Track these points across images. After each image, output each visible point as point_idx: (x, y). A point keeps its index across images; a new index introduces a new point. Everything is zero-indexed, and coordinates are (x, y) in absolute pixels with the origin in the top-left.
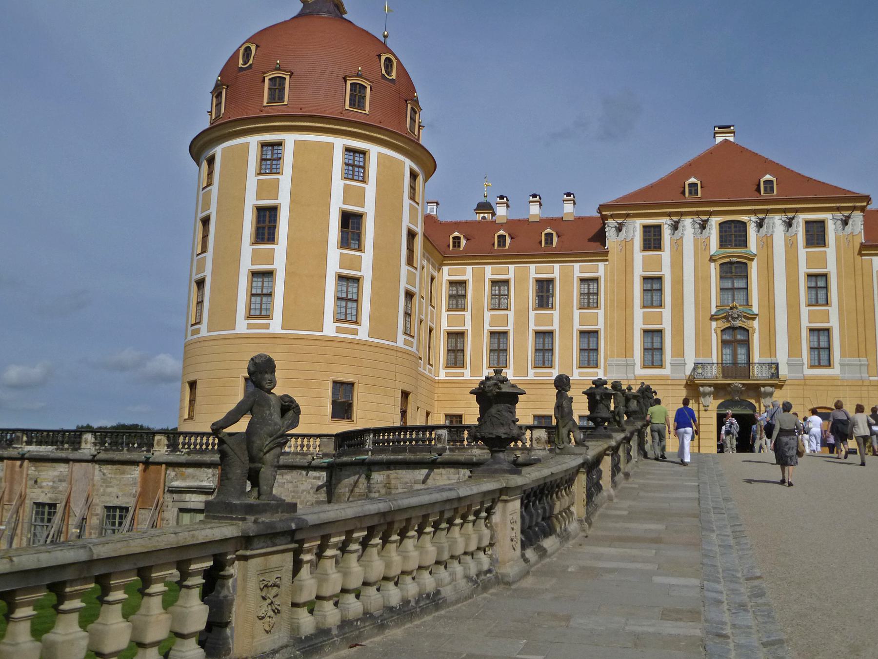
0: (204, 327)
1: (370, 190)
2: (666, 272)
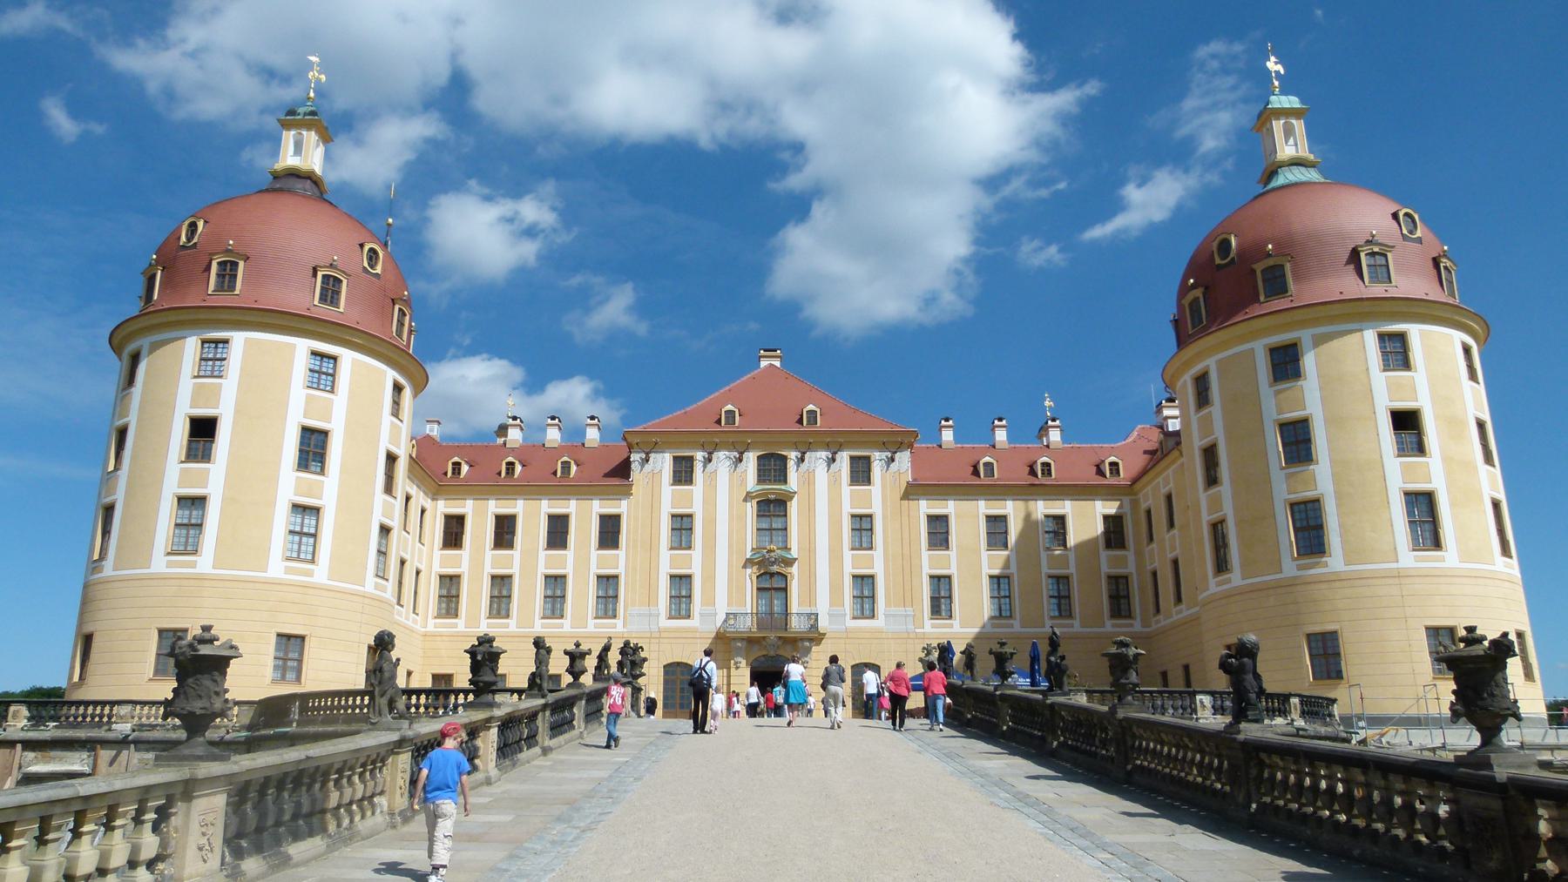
2: (697, 510)
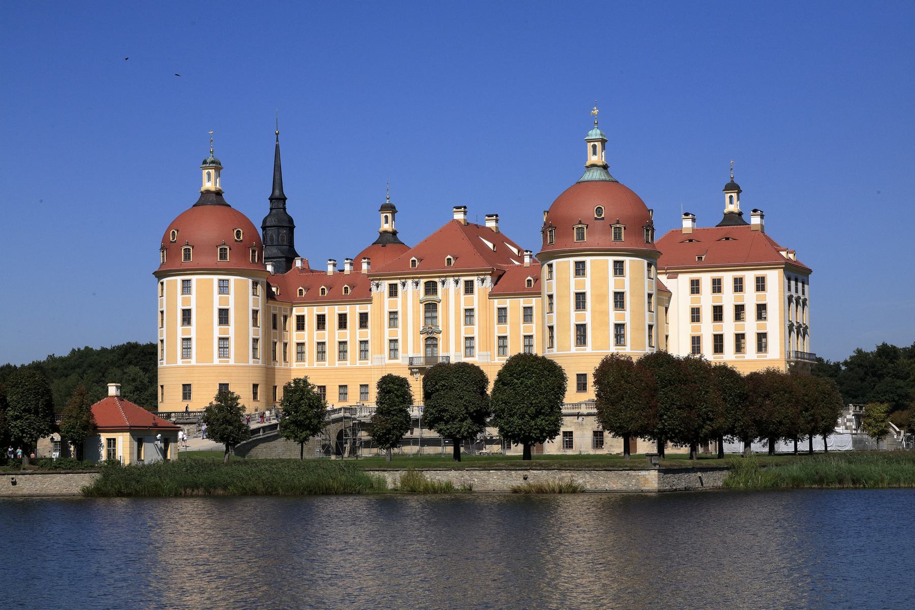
0: (164, 361)
1: (231, 297)
2: (399, 309)
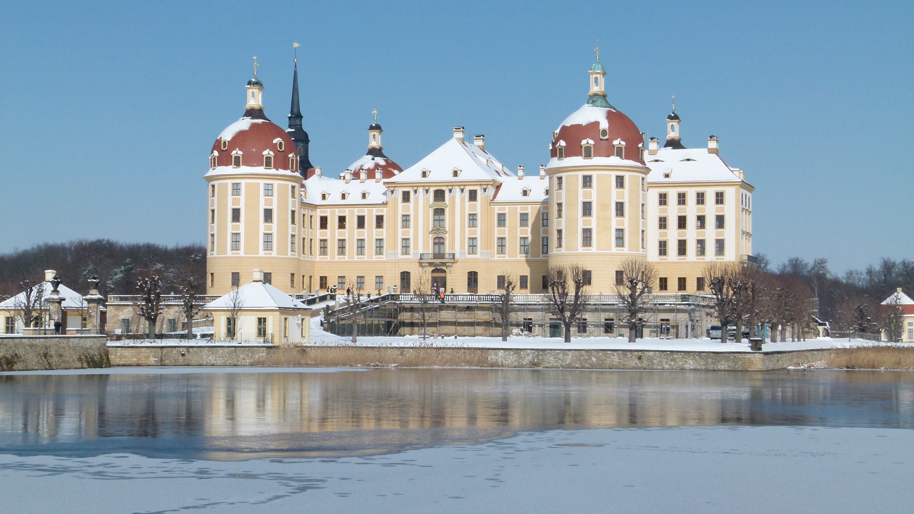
0: (215, 252)
1: (275, 199)
2: (411, 213)
